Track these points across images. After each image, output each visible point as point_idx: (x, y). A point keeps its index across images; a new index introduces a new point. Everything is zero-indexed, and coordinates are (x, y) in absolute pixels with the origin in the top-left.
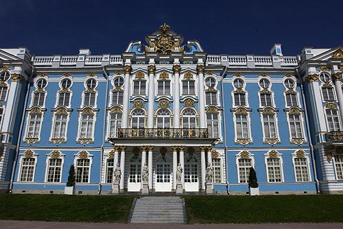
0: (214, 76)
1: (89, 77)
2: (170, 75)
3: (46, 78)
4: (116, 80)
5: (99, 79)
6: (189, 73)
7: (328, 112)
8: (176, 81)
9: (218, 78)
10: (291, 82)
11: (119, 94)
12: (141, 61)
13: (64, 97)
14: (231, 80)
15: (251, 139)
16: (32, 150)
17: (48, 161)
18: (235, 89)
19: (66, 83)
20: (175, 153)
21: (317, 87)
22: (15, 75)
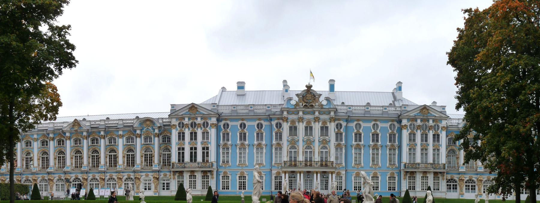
0: (341, 122)
1: (257, 122)
2: (312, 123)
3: (228, 122)
4: (277, 124)
5: (264, 123)
6: (324, 122)
7: (410, 149)
8: (317, 127)
9: (344, 124)
10: (394, 125)
11: (279, 136)
12: (293, 113)
13: (243, 137)
14: (353, 125)
15: (363, 164)
16: (227, 171)
17: (238, 178)
18: (355, 131)
19: (243, 126)
20: (315, 175)
21: (405, 134)
22: (213, 124)
